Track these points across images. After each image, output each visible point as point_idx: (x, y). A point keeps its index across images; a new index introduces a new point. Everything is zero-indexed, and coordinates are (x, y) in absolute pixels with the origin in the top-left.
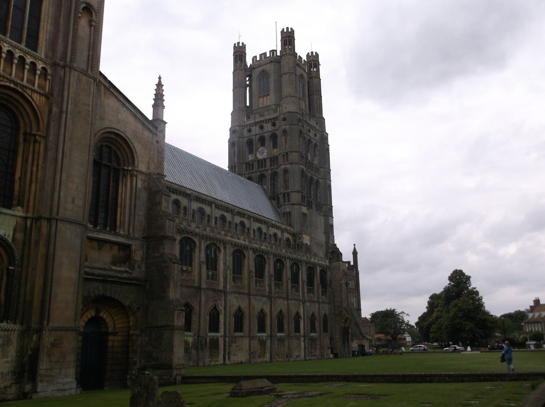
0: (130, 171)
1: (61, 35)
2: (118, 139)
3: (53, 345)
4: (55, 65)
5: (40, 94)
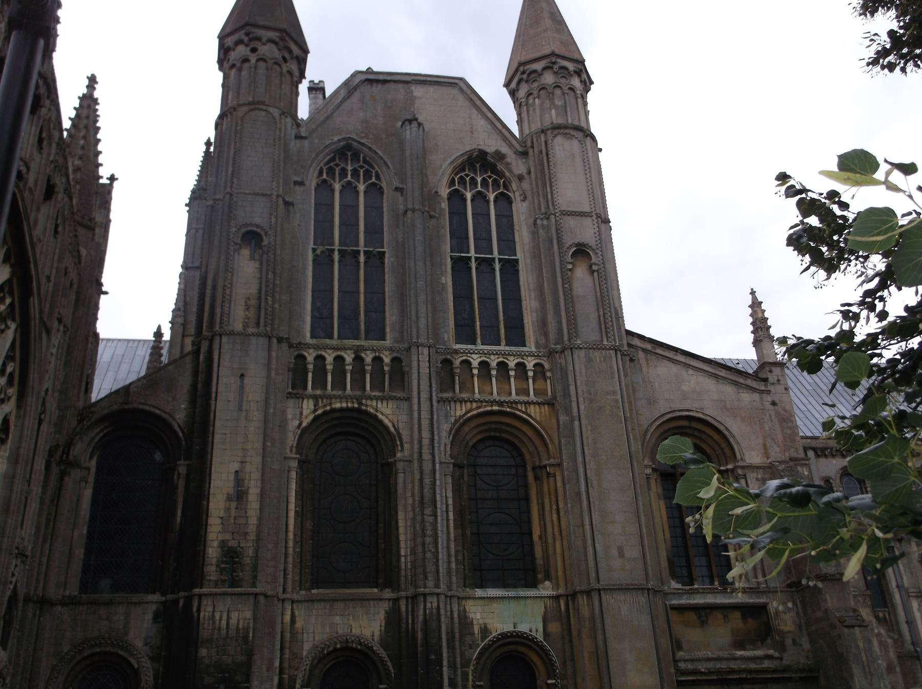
0: (733, 470)
1: (550, 307)
2: (694, 425)
4: (551, 354)
5: (539, 404)
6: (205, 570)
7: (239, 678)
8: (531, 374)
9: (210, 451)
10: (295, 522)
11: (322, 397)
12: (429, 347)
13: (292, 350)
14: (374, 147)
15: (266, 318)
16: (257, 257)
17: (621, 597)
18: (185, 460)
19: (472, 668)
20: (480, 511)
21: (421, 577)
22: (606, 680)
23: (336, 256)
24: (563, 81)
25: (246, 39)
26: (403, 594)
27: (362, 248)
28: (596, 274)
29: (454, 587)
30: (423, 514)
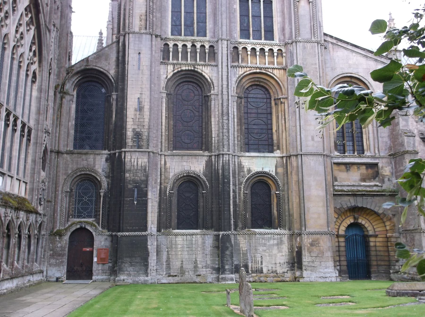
1: (287, 21)
3: (312, 245)
4: (286, 44)
5: (279, 69)
7: (143, 186)
8: (275, 54)
9: (126, 88)
10: (165, 121)
13: (162, 41)
17: (311, 158)
18: (115, 92)
19: (243, 185)
21: (222, 147)
22: (302, 192)
26: (213, 154)
28: (311, 4)
29: (236, 151)
30: (223, 119)
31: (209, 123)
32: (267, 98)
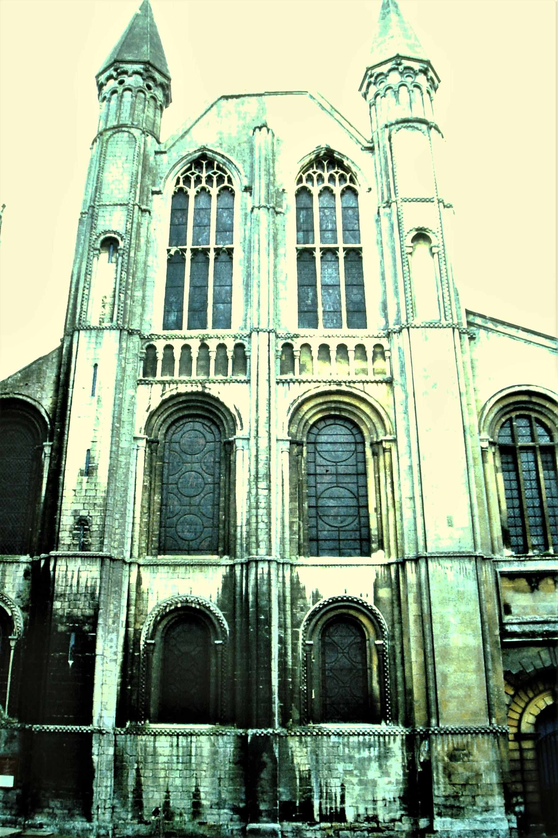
2: (534, 400)
3: (453, 757)
6: (60, 535)
7: (86, 628)
8: (370, 355)
9: (66, 432)
10: (143, 495)
11: (170, 382)
12: (269, 333)
13: (144, 341)
14: (226, 155)
15: (118, 313)
16: (114, 259)
17: (446, 563)
18: (50, 441)
19: (302, 628)
20: (318, 486)
21: (254, 545)
22: (428, 641)
23: (188, 255)
24: (409, 80)
25: (115, 74)
26: (238, 560)
27: (212, 246)
28: (436, 255)
29: (287, 555)
30: (257, 488)
31: (232, 496)
32: (356, 443)
